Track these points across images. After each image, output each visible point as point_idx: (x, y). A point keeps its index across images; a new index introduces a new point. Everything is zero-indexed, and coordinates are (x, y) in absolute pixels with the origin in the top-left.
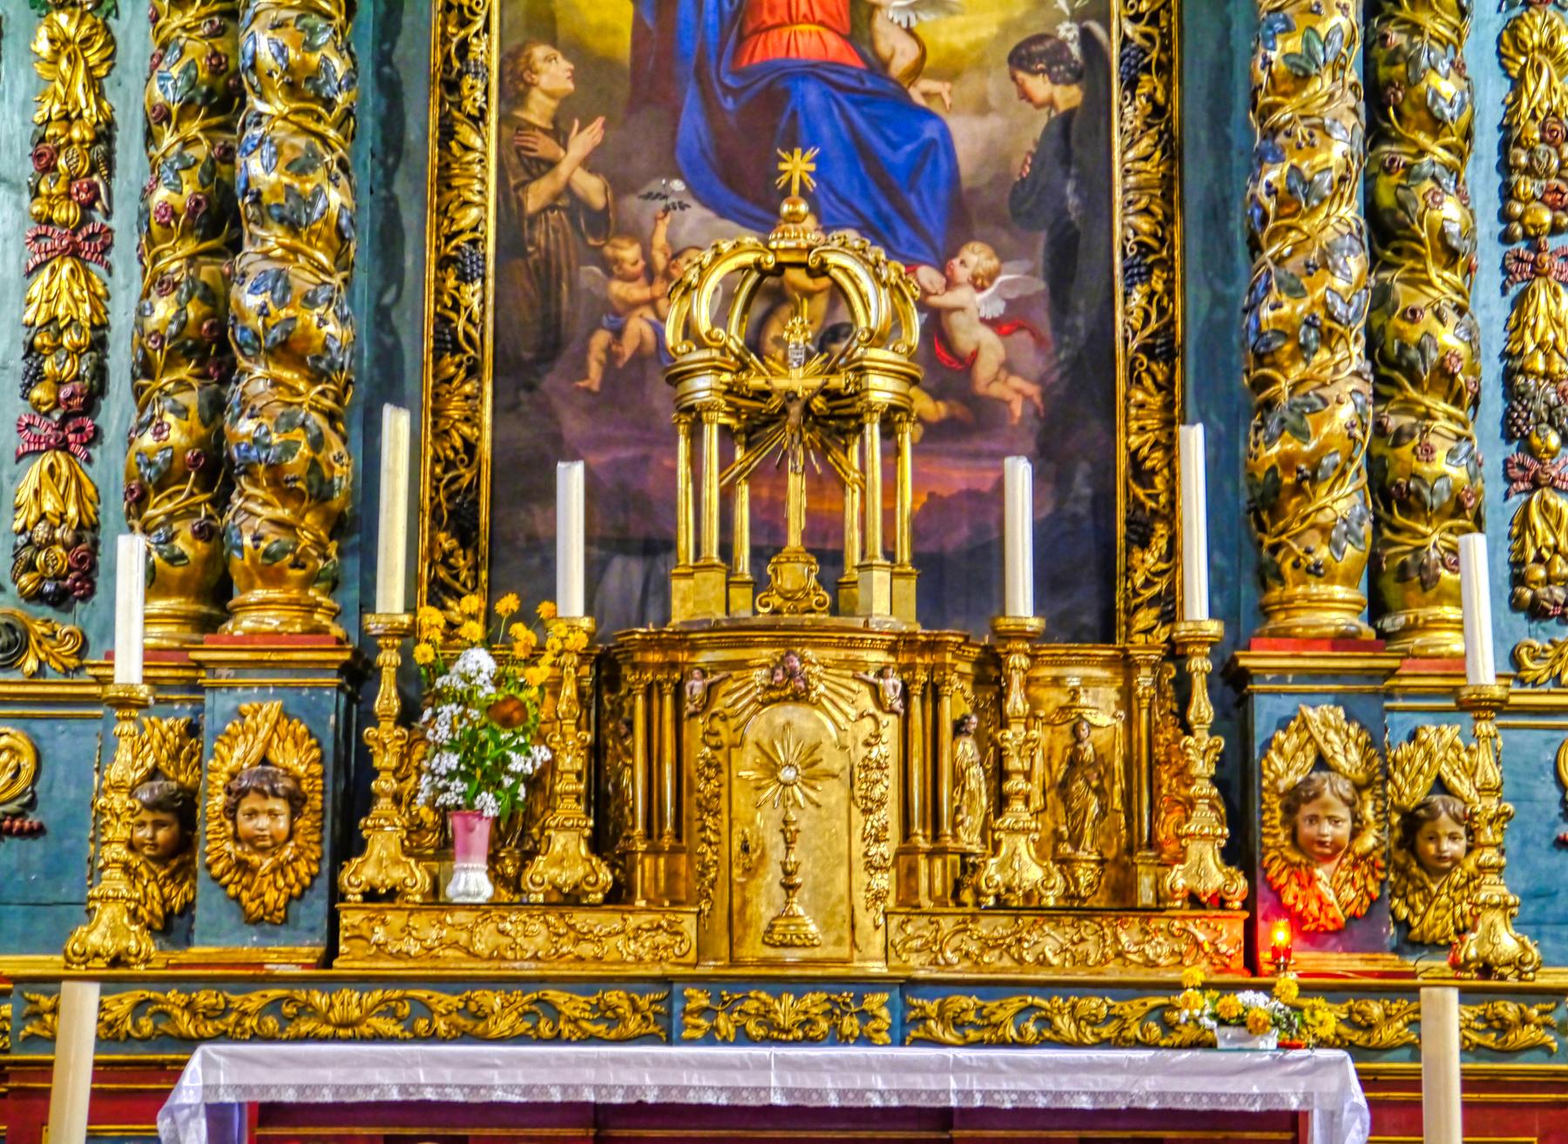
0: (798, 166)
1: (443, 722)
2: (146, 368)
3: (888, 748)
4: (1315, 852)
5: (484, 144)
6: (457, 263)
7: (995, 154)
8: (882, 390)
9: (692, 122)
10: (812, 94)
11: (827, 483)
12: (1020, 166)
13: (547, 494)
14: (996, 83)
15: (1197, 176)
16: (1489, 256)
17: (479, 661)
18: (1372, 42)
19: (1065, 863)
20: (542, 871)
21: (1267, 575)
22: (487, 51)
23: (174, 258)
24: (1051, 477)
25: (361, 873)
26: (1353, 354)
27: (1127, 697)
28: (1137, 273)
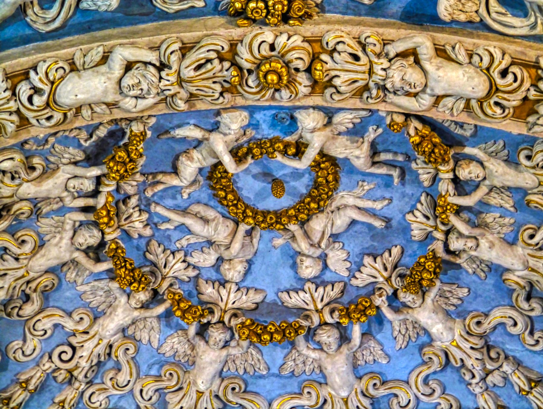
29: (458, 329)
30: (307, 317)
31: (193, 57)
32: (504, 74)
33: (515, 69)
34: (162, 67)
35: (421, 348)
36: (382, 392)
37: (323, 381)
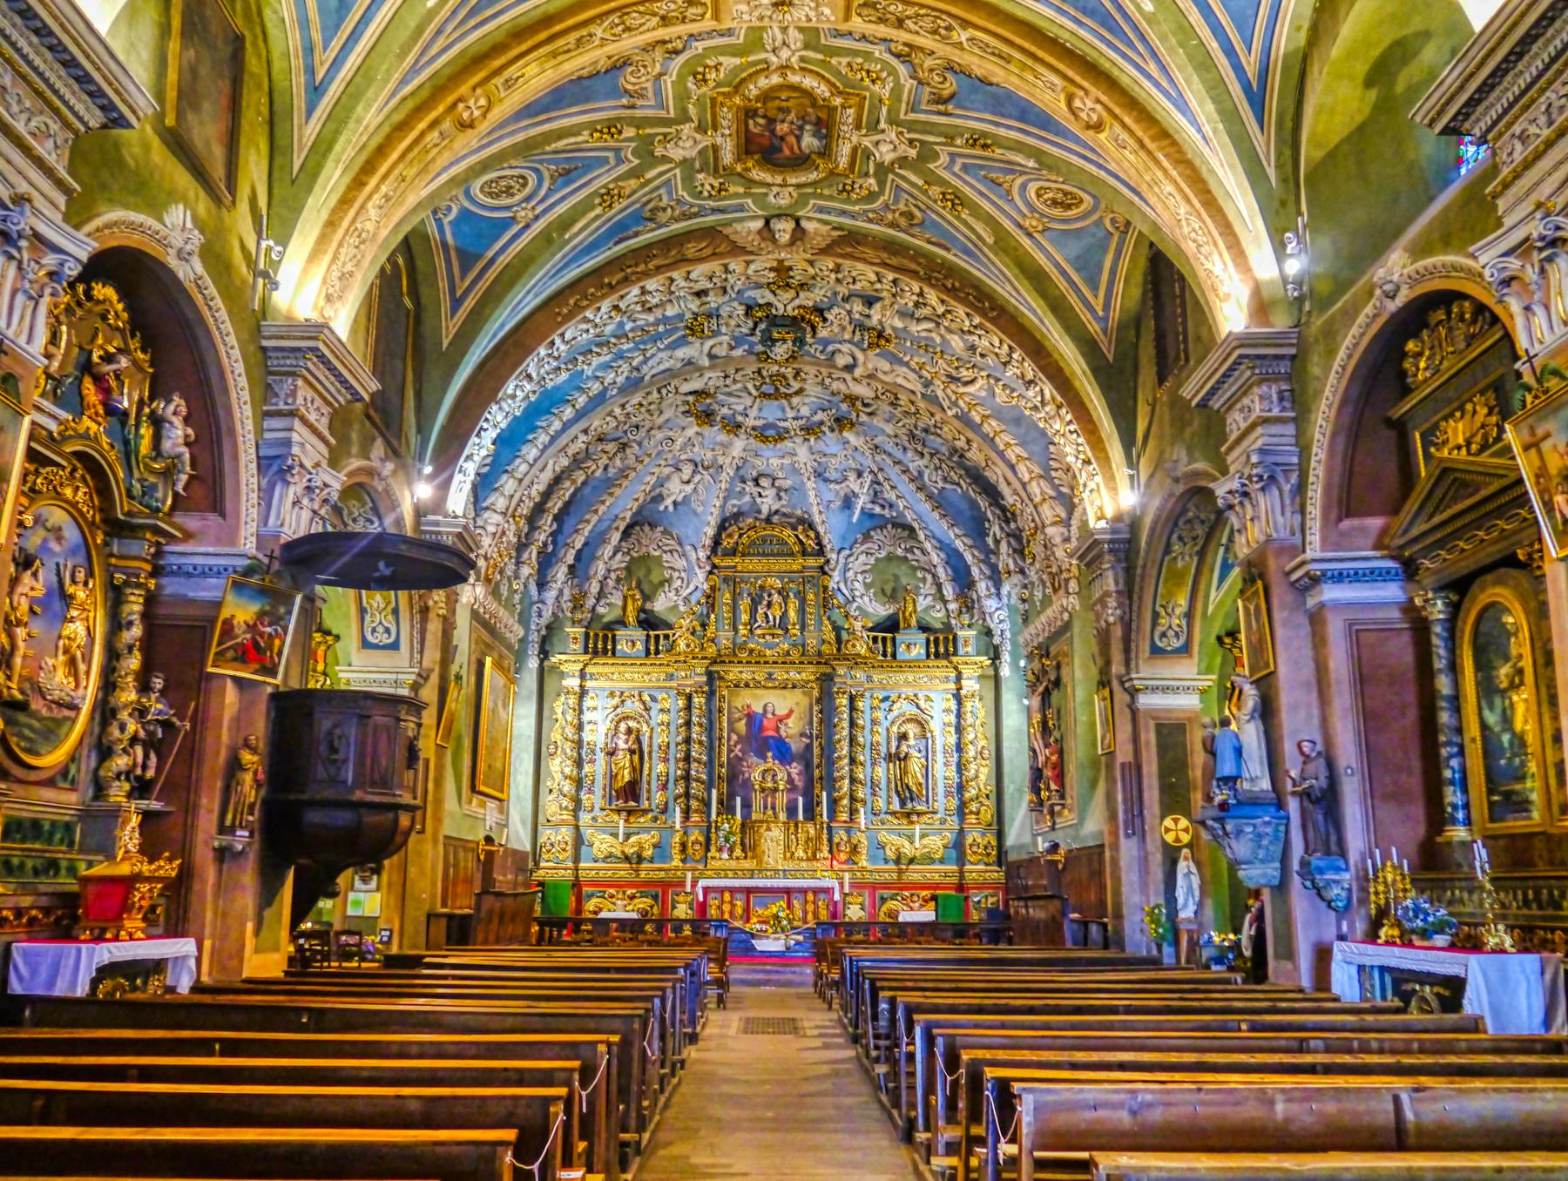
0: (770, 754)
1: (721, 834)
6: (722, 766)
11: (774, 798)
16: (868, 764)
24: (804, 796)
26: (847, 781)
34: (726, 377)
37: (794, 455)
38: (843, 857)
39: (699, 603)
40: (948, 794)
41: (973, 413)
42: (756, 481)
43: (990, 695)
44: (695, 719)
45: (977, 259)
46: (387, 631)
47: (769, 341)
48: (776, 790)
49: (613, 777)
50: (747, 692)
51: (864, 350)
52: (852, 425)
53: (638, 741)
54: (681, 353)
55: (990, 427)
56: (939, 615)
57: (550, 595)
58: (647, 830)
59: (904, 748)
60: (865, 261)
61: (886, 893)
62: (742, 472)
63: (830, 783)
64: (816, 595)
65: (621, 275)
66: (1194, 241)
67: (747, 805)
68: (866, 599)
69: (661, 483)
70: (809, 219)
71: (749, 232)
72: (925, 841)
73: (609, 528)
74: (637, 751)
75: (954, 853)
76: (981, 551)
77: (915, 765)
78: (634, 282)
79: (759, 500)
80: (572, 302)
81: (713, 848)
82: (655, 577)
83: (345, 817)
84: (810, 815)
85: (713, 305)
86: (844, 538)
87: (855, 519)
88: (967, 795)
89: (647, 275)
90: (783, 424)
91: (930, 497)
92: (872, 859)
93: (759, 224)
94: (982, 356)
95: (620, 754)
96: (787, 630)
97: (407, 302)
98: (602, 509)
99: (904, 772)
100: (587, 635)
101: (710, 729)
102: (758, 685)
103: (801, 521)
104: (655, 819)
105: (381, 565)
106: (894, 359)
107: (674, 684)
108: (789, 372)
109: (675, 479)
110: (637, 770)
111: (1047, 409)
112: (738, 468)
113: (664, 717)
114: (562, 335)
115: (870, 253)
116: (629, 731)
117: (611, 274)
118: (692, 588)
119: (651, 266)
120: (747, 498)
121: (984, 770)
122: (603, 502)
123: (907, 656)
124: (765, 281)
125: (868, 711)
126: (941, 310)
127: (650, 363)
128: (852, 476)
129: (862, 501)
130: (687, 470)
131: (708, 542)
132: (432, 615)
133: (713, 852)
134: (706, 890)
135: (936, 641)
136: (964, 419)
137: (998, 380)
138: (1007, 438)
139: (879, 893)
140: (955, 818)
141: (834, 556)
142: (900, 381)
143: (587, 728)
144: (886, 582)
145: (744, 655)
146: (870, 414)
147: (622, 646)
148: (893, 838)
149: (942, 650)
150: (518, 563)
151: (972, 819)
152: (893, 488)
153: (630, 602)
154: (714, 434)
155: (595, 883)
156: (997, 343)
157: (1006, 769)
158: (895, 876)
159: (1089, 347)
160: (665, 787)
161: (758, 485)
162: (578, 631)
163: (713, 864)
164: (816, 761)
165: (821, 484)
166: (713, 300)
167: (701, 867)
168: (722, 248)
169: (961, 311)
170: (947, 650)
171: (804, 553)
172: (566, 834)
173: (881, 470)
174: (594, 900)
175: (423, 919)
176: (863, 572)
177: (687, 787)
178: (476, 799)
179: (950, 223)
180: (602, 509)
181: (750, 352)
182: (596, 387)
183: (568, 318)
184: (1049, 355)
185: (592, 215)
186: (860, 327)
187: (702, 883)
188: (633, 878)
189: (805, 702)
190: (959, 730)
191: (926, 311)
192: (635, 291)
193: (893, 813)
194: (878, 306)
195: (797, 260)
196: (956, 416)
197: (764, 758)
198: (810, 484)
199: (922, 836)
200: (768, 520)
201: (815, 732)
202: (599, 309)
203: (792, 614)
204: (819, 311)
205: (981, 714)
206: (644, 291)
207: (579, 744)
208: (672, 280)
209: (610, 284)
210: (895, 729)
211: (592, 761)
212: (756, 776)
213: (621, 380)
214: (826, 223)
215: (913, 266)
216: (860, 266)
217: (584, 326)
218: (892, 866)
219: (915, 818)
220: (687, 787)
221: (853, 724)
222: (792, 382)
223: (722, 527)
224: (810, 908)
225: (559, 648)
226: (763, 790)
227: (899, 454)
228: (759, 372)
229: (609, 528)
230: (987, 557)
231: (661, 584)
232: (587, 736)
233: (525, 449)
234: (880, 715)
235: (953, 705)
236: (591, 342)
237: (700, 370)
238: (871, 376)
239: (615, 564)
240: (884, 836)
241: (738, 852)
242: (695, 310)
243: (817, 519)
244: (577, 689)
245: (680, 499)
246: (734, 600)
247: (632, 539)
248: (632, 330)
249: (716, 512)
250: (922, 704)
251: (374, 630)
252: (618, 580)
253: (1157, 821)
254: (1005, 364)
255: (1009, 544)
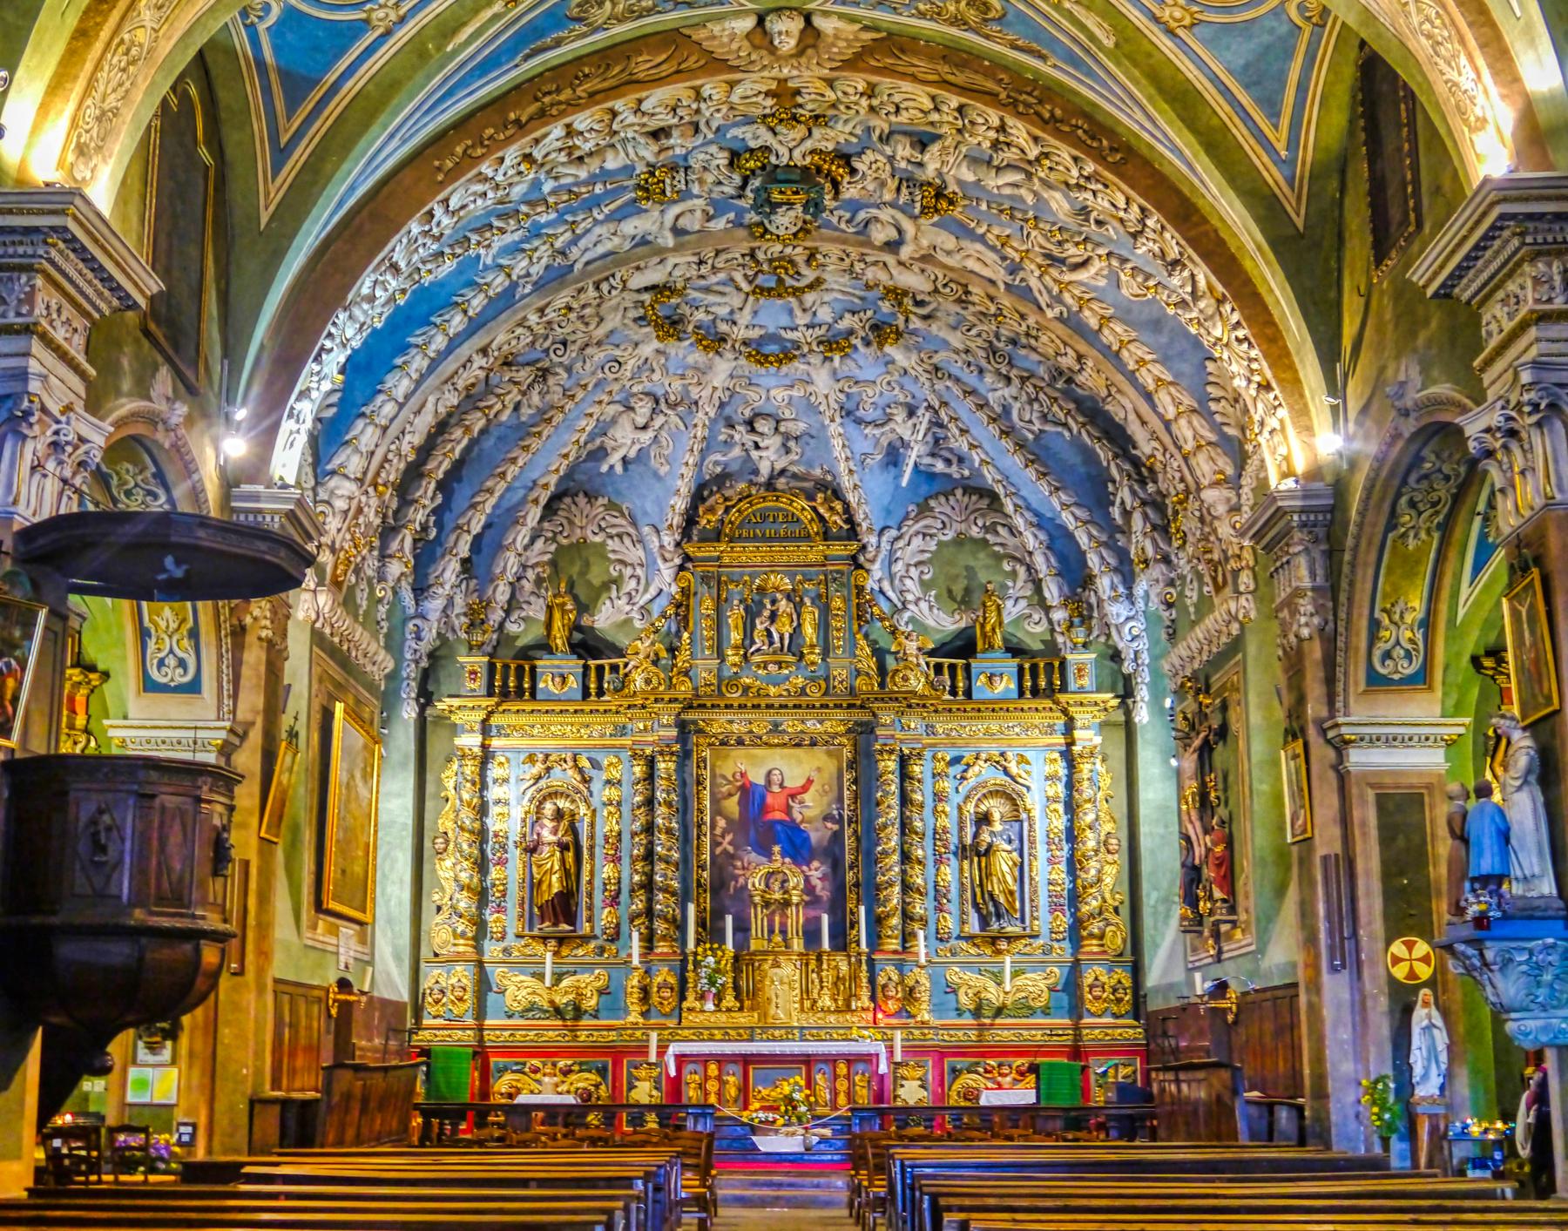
0: (777, 849)
1: (703, 972)
2: (633, 891)
3: (797, 977)
4: (888, 998)
5: (707, 840)
6: (702, 867)
7: (820, 841)
8: (795, 899)
9: (752, 833)
10: (779, 827)
11: (784, 916)
12: (825, 843)
13: (723, 919)
14: (819, 824)
15: (864, 844)
16: (930, 862)
17: (711, 959)
18: (902, 813)
19: (836, 1001)
20: (725, 1004)
21: (880, 937)
22: (708, 819)
23: (639, 866)
24: (832, 913)
25: (685, 1005)
26: (897, 889)
27: (850, 964)
28: (851, 868)
29: (914, 357)
30: (799, 348)
31: (724, 257)
32: (945, 285)
33: (953, 285)
34: (701, 262)
35: (887, 364)
36: (854, 390)
37: (810, 382)
38: (892, 1006)
39: (664, 615)
40: (1054, 908)
41: (1087, 313)
42: (750, 424)
43: (1119, 754)
44: (660, 795)
45: (1090, 73)
46: (182, 663)
47: (767, 205)
48: (787, 903)
49: (534, 886)
50: (740, 752)
51: (915, 218)
52: (899, 334)
53: (573, 830)
54: (631, 227)
55: (1114, 334)
56: (1038, 629)
57: (434, 606)
58: (589, 967)
59: (985, 837)
60: (914, 78)
61: (960, 1063)
62: (728, 411)
63: (871, 892)
64: (846, 600)
65: (533, 108)
66: (1429, 36)
67: (742, 928)
68: (924, 605)
69: (603, 429)
70: (826, 14)
71: (733, 37)
72: (1020, 981)
73: (524, 501)
74: (572, 846)
75: (1065, 998)
76: (1101, 529)
77: (1003, 863)
78: (555, 118)
79: (755, 454)
80: (459, 150)
81: (691, 996)
82: (596, 577)
83: (118, 952)
84: (841, 941)
85: (678, 151)
86: (888, 512)
87: (904, 482)
88: (1085, 909)
89: (574, 106)
90: (790, 335)
91: (1021, 445)
92: (937, 1009)
93: (749, 23)
94: (1099, 223)
95: (546, 851)
96: (801, 656)
97: (204, 153)
98: (512, 471)
99: (986, 874)
100: (491, 668)
101: (683, 810)
102: (758, 742)
103: (822, 486)
104: (601, 950)
105: (169, 561)
106: (963, 231)
107: (627, 741)
108: (799, 254)
109: (625, 421)
110: (571, 876)
111: (1202, 304)
112: (722, 405)
113: (613, 793)
114: (446, 201)
115: (921, 65)
116: (559, 815)
117: (518, 105)
118: (653, 591)
119: (579, 91)
120: (737, 452)
121: (1110, 870)
122: (514, 461)
123: (988, 694)
124: (760, 112)
125: (928, 780)
126: (1033, 152)
127: (582, 243)
128: (900, 415)
129: (916, 453)
130: (643, 410)
131: (677, 520)
132: (250, 638)
133: (691, 1001)
134: (681, 1059)
135: (1034, 668)
136: (1072, 322)
137: (1124, 261)
138: (1140, 351)
139: (947, 1062)
140: (1066, 945)
141: (873, 540)
142: (971, 264)
143: (494, 810)
144: (955, 578)
145: (734, 696)
146: (926, 318)
147: (546, 684)
148: (970, 976)
149: (1043, 683)
150: (384, 557)
151: (1092, 946)
152: (963, 432)
153: (557, 615)
154: (684, 352)
155: (508, 1051)
156: (1122, 203)
157: (1146, 867)
158: (973, 1035)
159: (1265, 206)
160: (614, 901)
161: (753, 430)
162: (479, 661)
163: (689, 1019)
164: (848, 858)
165: (852, 427)
166: (678, 143)
167: (672, 1023)
168: (690, 63)
169: (1065, 153)
170: (1050, 683)
171: (826, 536)
172: (462, 975)
173: (945, 404)
174: (508, 1077)
175: (243, 1106)
176: (915, 565)
177: (650, 901)
178: (323, 923)
179: (1046, 17)
180: (512, 471)
181: (738, 223)
182: (499, 282)
183: (453, 175)
184: (1205, 221)
185: (487, 14)
186: (908, 181)
187: (674, 1049)
188: (565, 1040)
189: (831, 766)
190: (1071, 807)
191: (1010, 155)
192: (557, 131)
193: (970, 938)
194: (935, 148)
195: (808, 77)
196: (1060, 319)
197: (768, 854)
198: (834, 428)
199: (1015, 974)
200: (770, 485)
201: (846, 813)
202: (502, 160)
203: (809, 631)
204: (845, 158)
205: (1106, 782)
206: (570, 132)
207: (481, 835)
208: (614, 114)
209: (517, 122)
210: (971, 807)
211: (502, 862)
212: (756, 882)
213: (537, 270)
214: (852, 20)
215: (990, 85)
216: (907, 86)
217: (479, 188)
218: (968, 1020)
219: (1003, 945)
220: (650, 901)
221: (905, 800)
222: (804, 270)
223: (698, 497)
224: (842, 1085)
225: (445, 689)
226: (767, 904)
227: (971, 379)
228: (752, 255)
229: (524, 501)
230: (1111, 537)
231: (606, 586)
232: (494, 824)
233: (390, 380)
234: (947, 785)
235: (1061, 769)
236: (489, 214)
237: (661, 253)
238: (927, 258)
239: (533, 556)
240: (955, 974)
241: (729, 1000)
242: (652, 159)
243: (846, 482)
244: (477, 751)
245: (632, 454)
246: (718, 610)
247: (559, 519)
248: (554, 192)
249: (688, 473)
250: (1013, 768)
251: (161, 663)
252: (539, 581)
253: (1381, 945)
254: (1135, 236)
255: (1146, 517)
